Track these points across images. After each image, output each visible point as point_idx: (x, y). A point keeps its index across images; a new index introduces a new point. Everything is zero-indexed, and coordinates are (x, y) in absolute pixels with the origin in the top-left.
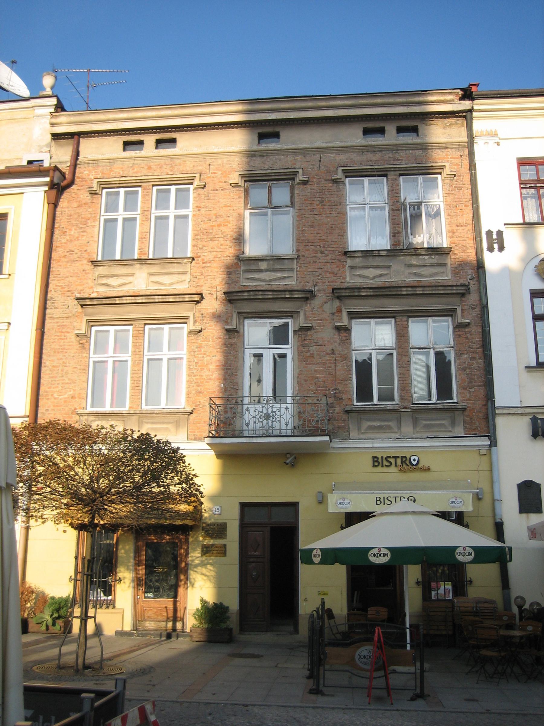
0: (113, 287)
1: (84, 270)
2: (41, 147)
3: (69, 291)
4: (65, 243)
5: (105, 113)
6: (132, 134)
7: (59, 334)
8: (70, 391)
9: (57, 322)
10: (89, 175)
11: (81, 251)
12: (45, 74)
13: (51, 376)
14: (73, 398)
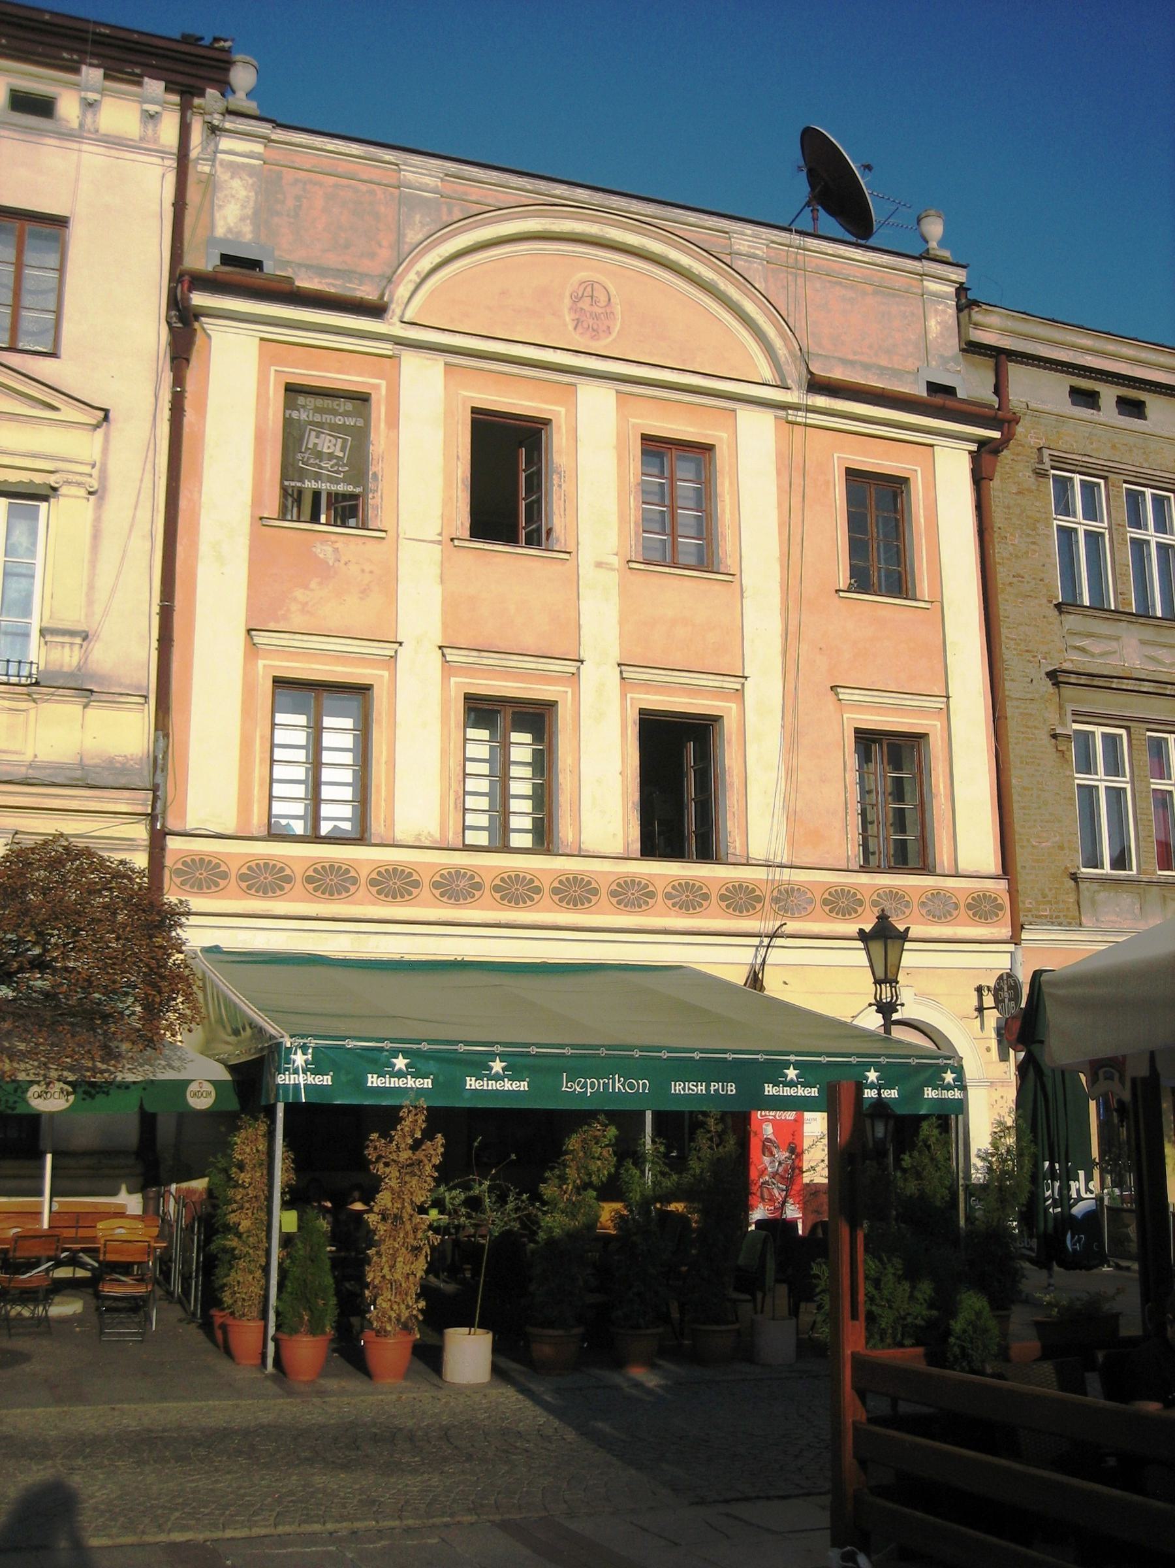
0: (1093, 655)
1: (1044, 617)
2: (944, 360)
3: (1027, 651)
4: (1008, 559)
5: (1062, 330)
6: (1084, 377)
7: (1023, 730)
8: (1055, 836)
9: (1018, 707)
10: (1026, 437)
11: (1034, 579)
12: (932, 212)
13: (1022, 805)
14: (1061, 848)
